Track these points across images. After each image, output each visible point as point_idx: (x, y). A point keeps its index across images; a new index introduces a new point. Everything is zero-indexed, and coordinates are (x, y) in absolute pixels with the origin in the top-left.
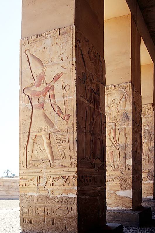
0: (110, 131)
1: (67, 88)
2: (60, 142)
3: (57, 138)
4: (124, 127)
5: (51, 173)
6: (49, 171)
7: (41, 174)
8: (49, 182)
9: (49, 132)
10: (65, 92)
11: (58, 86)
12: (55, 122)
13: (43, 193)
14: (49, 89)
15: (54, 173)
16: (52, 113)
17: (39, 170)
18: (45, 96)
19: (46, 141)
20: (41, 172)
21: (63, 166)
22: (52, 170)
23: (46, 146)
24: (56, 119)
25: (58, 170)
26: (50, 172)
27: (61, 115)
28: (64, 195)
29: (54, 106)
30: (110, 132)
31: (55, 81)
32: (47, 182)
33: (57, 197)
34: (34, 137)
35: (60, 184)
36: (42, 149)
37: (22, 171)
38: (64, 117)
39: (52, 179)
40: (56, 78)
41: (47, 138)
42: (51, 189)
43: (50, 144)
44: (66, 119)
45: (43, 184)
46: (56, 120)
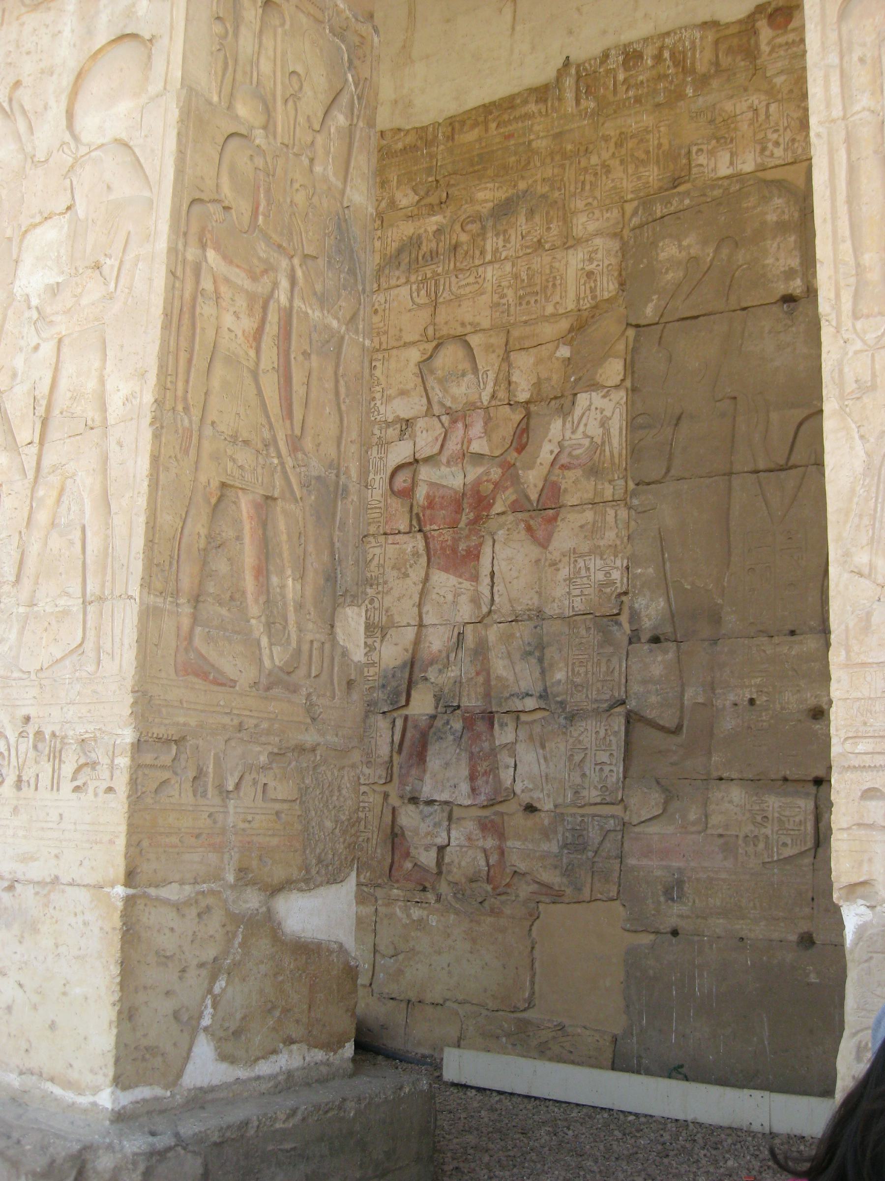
0: (265, 308)
4: (335, 324)
30: (263, 320)
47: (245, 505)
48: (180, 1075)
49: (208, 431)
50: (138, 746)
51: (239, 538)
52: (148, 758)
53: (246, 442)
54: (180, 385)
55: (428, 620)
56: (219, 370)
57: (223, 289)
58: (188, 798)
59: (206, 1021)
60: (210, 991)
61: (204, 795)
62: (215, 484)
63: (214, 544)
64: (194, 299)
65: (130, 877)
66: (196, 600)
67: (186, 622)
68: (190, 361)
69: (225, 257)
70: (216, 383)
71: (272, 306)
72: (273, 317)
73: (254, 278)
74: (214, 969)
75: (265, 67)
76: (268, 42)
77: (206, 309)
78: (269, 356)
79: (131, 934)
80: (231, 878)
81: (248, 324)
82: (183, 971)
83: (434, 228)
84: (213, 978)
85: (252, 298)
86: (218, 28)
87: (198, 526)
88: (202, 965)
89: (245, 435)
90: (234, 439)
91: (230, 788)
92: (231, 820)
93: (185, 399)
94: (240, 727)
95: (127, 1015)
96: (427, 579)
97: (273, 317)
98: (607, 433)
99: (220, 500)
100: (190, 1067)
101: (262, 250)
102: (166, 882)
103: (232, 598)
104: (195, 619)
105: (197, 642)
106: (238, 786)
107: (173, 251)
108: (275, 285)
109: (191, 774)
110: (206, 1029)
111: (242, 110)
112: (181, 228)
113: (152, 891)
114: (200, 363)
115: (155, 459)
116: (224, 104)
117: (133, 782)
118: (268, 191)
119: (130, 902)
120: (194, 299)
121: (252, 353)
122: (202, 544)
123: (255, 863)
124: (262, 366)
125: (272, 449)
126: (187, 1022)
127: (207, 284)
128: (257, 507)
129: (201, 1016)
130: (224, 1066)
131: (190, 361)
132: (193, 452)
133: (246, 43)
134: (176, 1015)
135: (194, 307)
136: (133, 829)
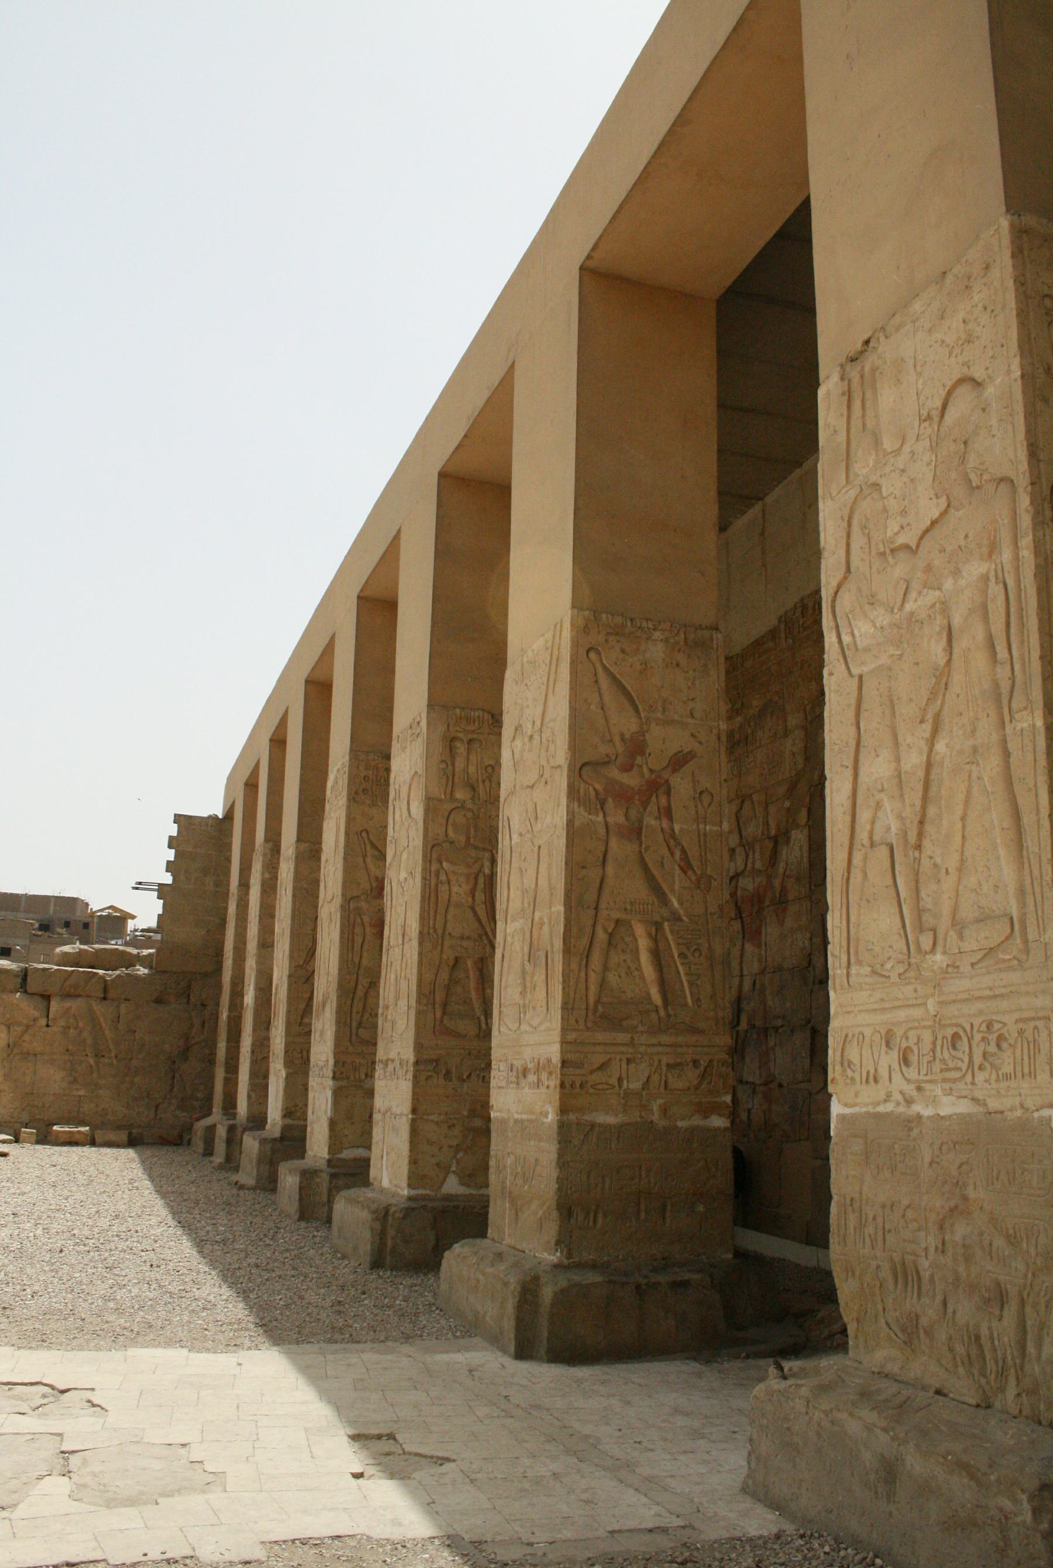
0: (476, 879)
1: (706, 799)
2: (686, 952)
3: (680, 941)
5: (660, 1049)
6: (654, 1041)
7: (631, 1050)
8: (655, 1078)
9: (657, 918)
10: (701, 810)
11: (681, 785)
12: (673, 891)
13: (638, 1114)
14: (656, 786)
15: (668, 1050)
16: (665, 862)
17: (622, 1037)
18: (645, 804)
19: (643, 943)
20: (632, 1043)
21: (693, 1030)
22: (665, 1039)
23: (645, 958)
24: (676, 885)
25: (681, 1039)
26: (660, 1044)
27: (690, 873)
28: (697, 1121)
29: (672, 843)
30: (476, 884)
31: (674, 771)
32: (649, 1077)
33: (676, 1127)
34: (612, 926)
35: (687, 1085)
36: (633, 969)
37: (571, 1036)
38: (698, 880)
39: (664, 1068)
40: (679, 761)
41: (649, 934)
42: (660, 1101)
43: (656, 954)
44: (702, 886)
45: (636, 1085)
46: (677, 883)
47: (470, 963)
48: (440, 1187)
49: (447, 937)
50: (417, 1063)
51: (467, 977)
52: (422, 1067)
53: (469, 938)
54: (431, 923)
55: (745, 973)
56: (452, 911)
57: (451, 877)
58: (442, 1081)
59: (453, 1168)
60: (455, 1157)
61: (451, 1080)
62: (452, 958)
63: (453, 981)
64: (437, 885)
65: (414, 1111)
66: (445, 1005)
67: (438, 1014)
68: (436, 912)
69: (451, 863)
70: (450, 917)
71: (481, 875)
72: (481, 880)
73: (468, 866)
74: (457, 1149)
75: (472, 769)
76: (473, 758)
77: (444, 888)
78: (480, 896)
79: (414, 1131)
80: (465, 1113)
81: (466, 888)
82: (441, 1148)
83: (738, 725)
84: (457, 1152)
85: (468, 876)
86: (443, 766)
87: (444, 975)
88: (451, 1147)
89: (467, 934)
90: (462, 938)
91: (465, 1077)
92: (465, 1090)
93: (434, 927)
94: (470, 1054)
95: (413, 1162)
96: (743, 945)
97: (481, 880)
98: (802, 856)
99: (454, 965)
100: (445, 1186)
101: (473, 853)
102: (431, 1114)
103: (465, 1002)
104: (444, 1013)
105: (445, 1022)
106: (469, 1076)
107: (424, 869)
108: (482, 866)
109: (444, 1072)
110: (454, 1172)
111: (459, 795)
112: (427, 859)
113: (425, 1117)
114: (441, 910)
115: (420, 954)
116: (448, 797)
117: (415, 1077)
118: (476, 827)
119: (413, 1120)
120: (437, 885)
121: (470, 899)
122: (446, 982)
123: (479, 1107)
124: (477, 902)
125: (484, 938)
126: (445, 1169)
127: (443, 878)
128: (475, 963)
129: (450, 1166)
130: (464, 1188)
131: (436, 912)
132: (439, 948)
133: (460, 763)
134: (438, 1165)
135: (437, 889)
136: (415, 1094)
